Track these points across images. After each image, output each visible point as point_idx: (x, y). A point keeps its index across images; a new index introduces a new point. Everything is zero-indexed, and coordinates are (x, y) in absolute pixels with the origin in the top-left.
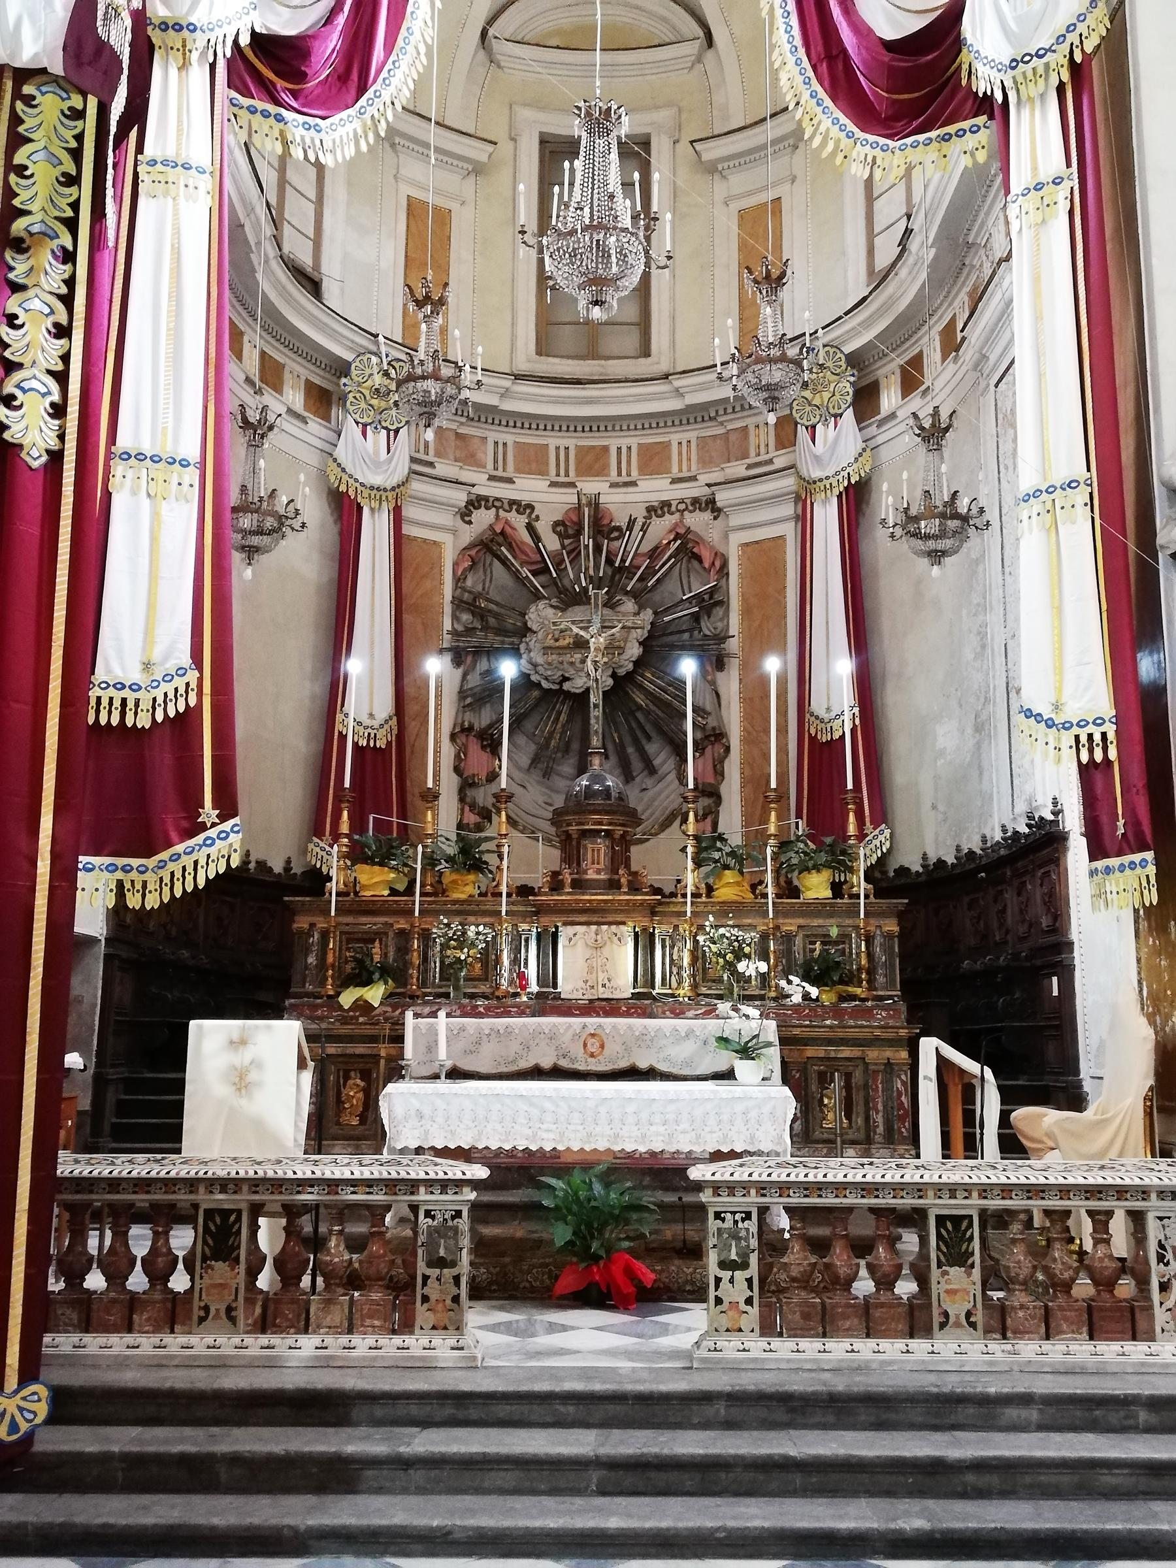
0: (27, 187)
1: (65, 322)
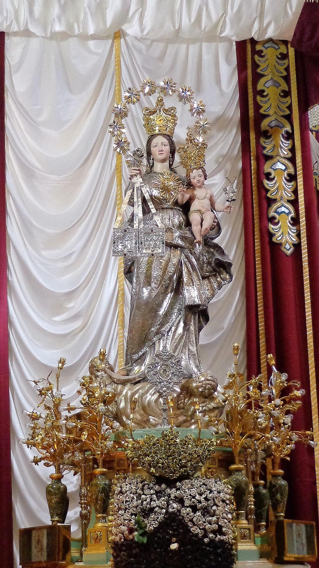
0: (266, 102)
1: (293, 173)
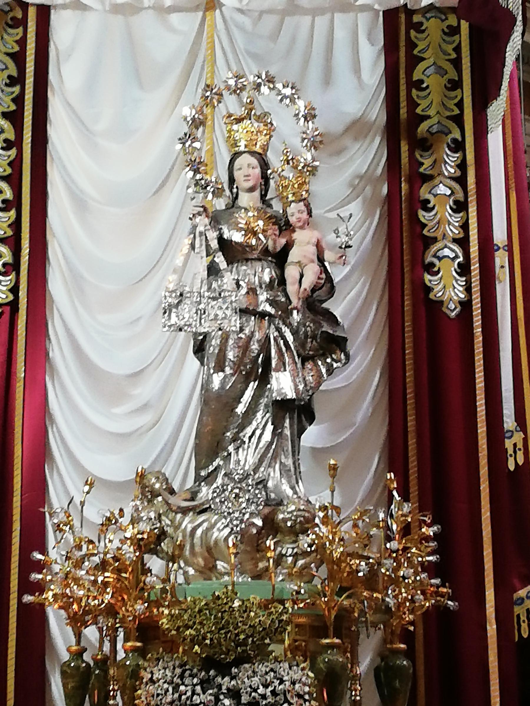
0: (425, 97)
1: (462, 199)
